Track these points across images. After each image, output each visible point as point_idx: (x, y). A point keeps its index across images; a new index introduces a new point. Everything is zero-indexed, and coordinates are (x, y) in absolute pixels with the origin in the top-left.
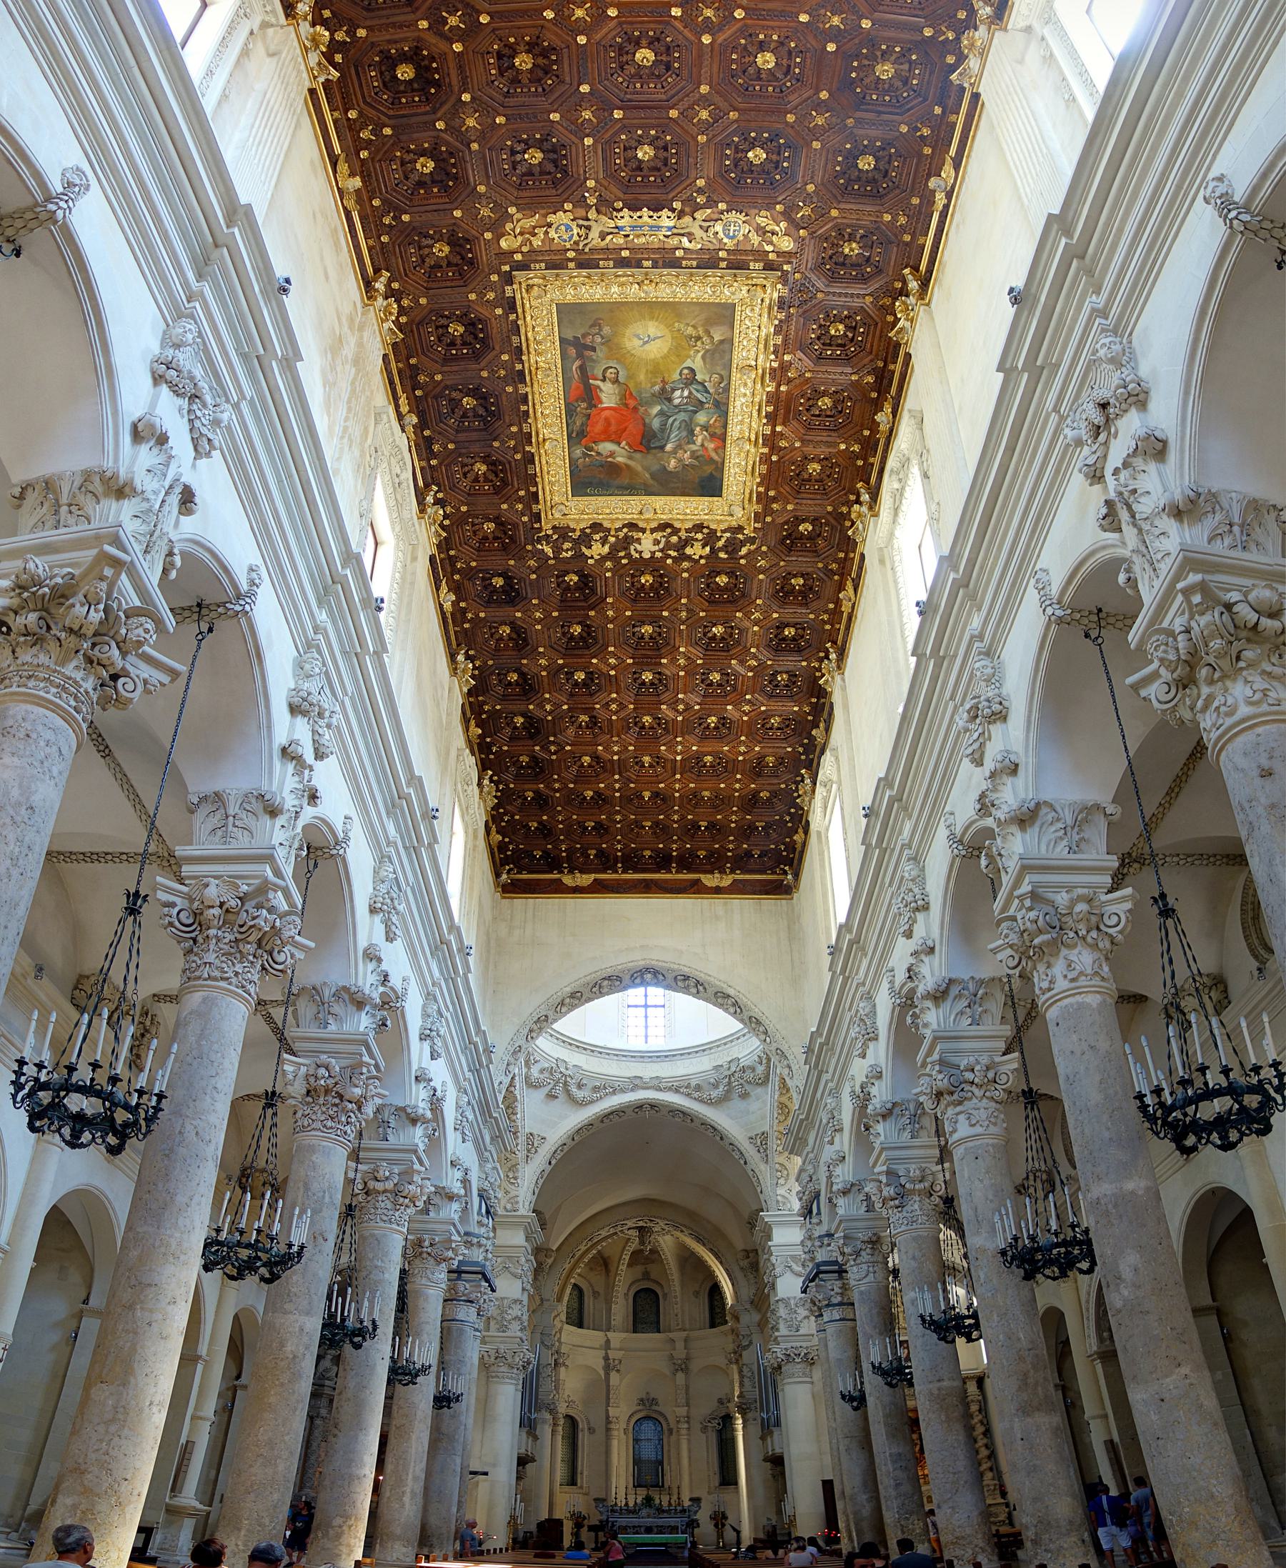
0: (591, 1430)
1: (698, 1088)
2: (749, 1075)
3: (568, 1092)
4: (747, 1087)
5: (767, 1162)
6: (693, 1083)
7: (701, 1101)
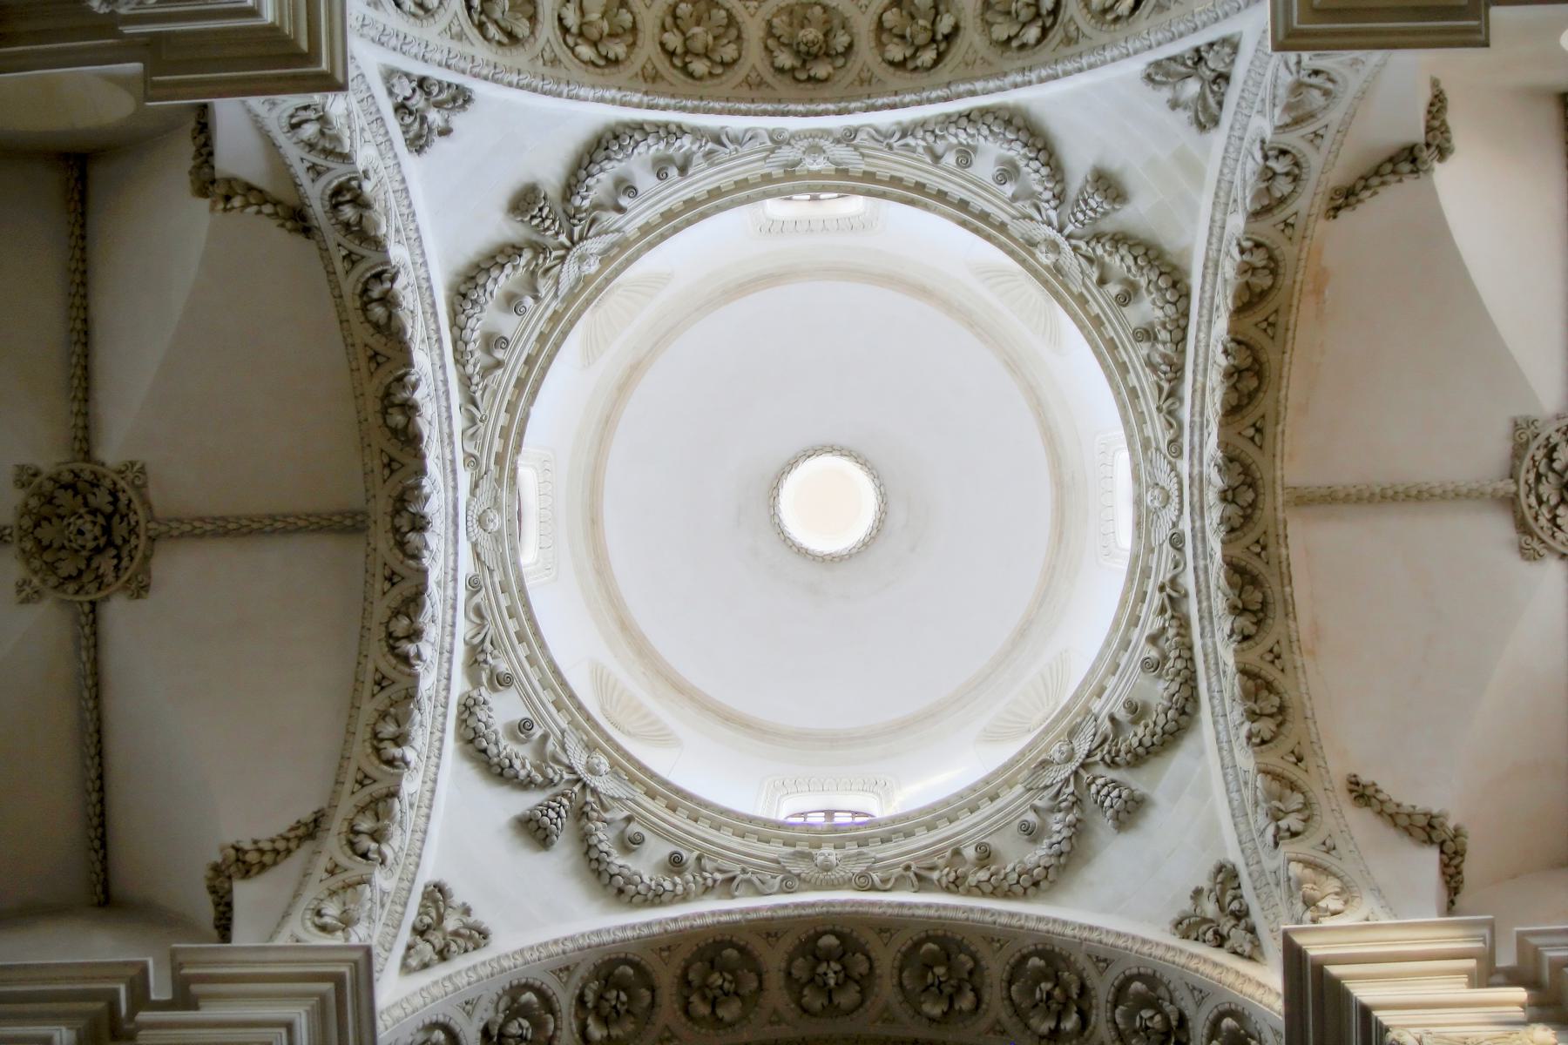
1: (986, 856)
2: (1134, 736)
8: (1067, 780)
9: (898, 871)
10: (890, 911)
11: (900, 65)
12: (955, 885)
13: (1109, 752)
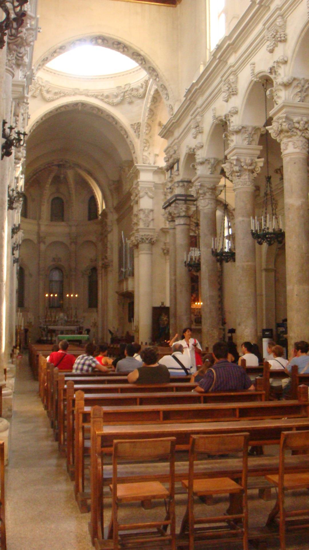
0: (31, 275)
1: (107, 97)
2: (134, 93)
3: (42, 94)
4: (134, 99)
5: (139, 137)
6: (105, 94)
7: (108, 103)
8: (122, 92)
12: (102, 100)
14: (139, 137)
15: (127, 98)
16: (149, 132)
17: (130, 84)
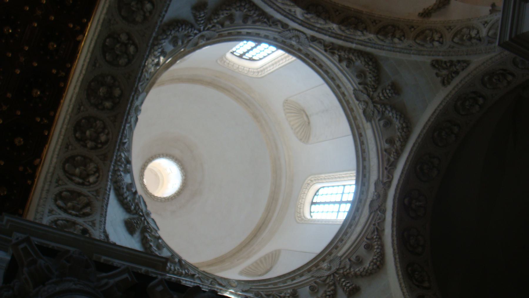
1: (390, 141)
2: (370, 79)
3: (356, 275)
6: (387, 146)
8: (375, 106)
9: (385, 172)
10: (403, 177)
11: (129, 62)
12: (398, 154)
13: (372, 88)
14: (464, 61)
15: (385, 95)
16: (437, 32)
17: (355, 90)
